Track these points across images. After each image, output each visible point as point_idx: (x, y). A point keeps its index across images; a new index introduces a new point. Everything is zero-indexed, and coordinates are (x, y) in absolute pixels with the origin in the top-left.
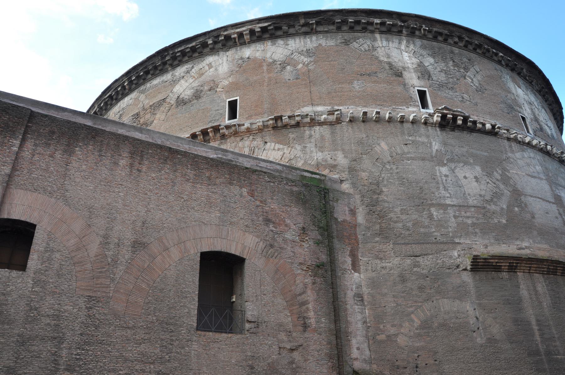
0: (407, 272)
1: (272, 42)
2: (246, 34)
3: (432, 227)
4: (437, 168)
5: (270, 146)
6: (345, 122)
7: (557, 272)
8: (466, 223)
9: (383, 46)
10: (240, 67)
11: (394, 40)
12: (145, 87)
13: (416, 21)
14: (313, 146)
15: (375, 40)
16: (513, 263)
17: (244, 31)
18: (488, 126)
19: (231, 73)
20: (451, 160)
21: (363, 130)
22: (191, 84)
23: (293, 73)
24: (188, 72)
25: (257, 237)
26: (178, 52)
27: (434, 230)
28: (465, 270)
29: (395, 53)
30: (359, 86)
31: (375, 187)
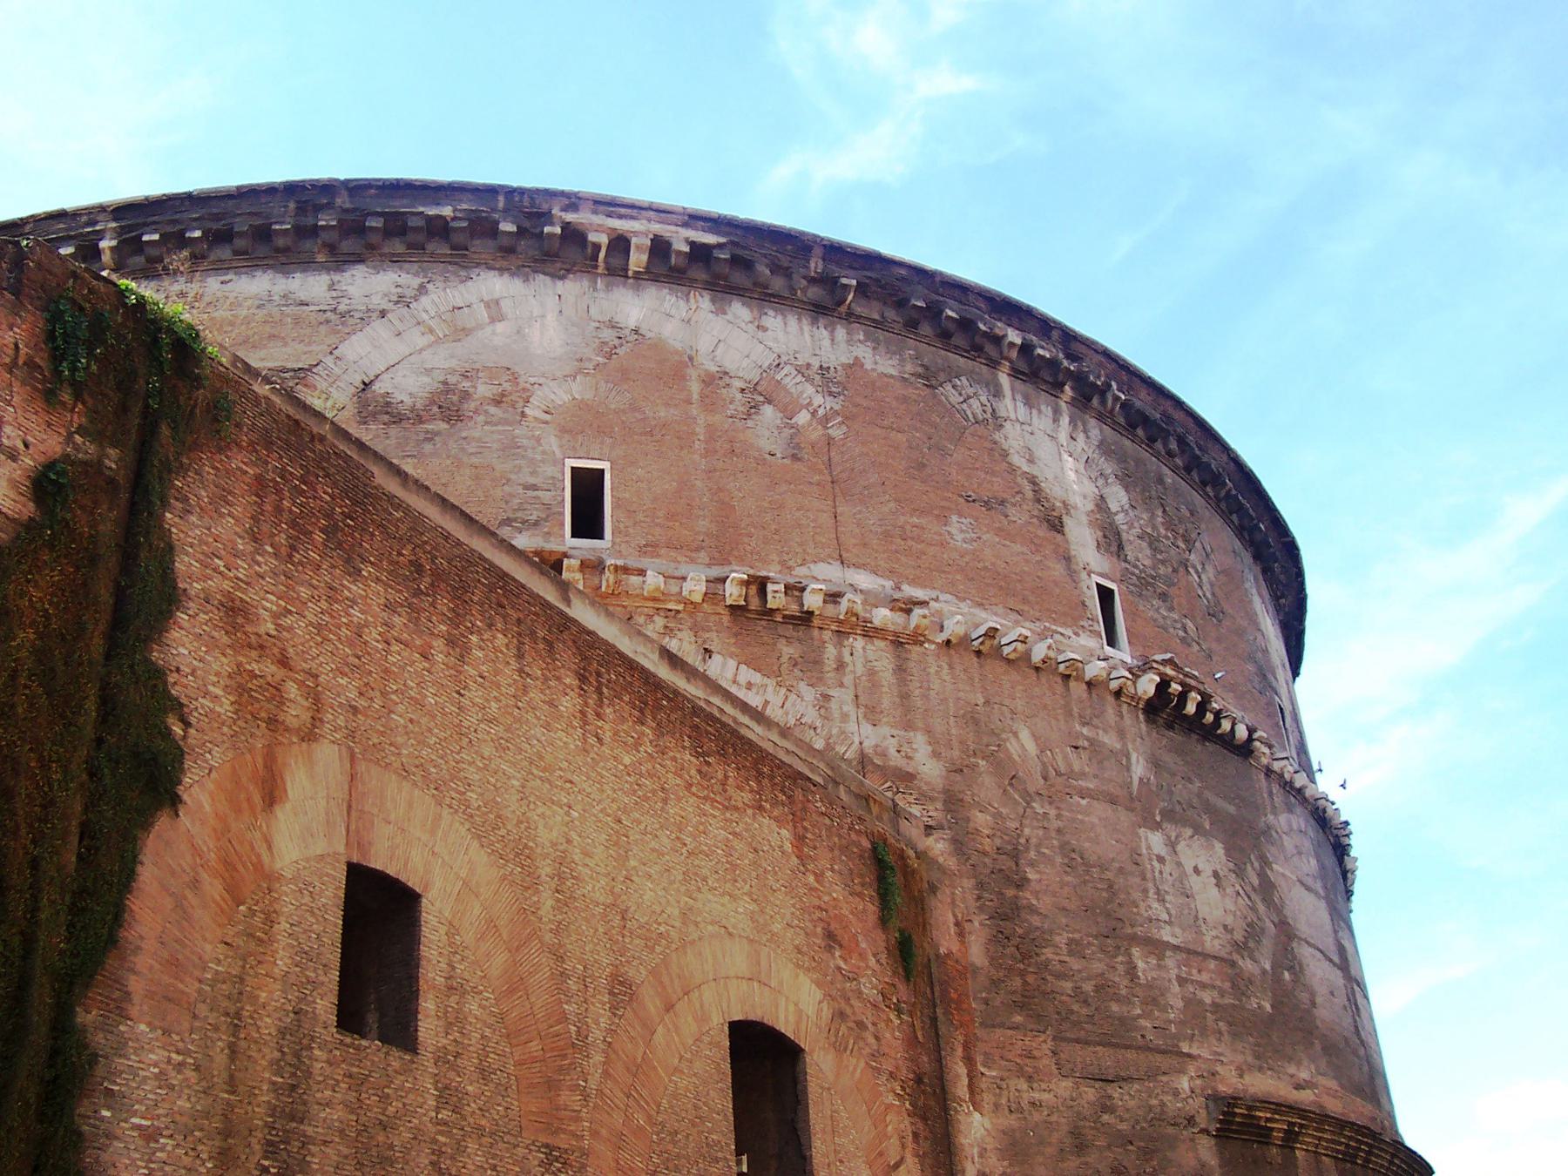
0: (1087, 1124)
1: (713, 301)
2: (637, 247)
3: (1134, 1004)
4: (1142, 831)
5: (724, 665)
6: (933, 642)
7: (1356, 1156)
8: (1201, 1002)
9: (1018, 420)
10: (609, 356)
11: (1043, 407)
13: (1100, 365)
14: (850, 701)
15: (997, 393)
16: (1294, 1124)
17: (635, 233)
18: (1242, 732)
20: (1169, 815)
21: (977, 680)
23: (783, 435)
24: (401, 301)
25: (818, 984)
29: (1044, 449)
30: (963, 536)
31: (1006, 863)
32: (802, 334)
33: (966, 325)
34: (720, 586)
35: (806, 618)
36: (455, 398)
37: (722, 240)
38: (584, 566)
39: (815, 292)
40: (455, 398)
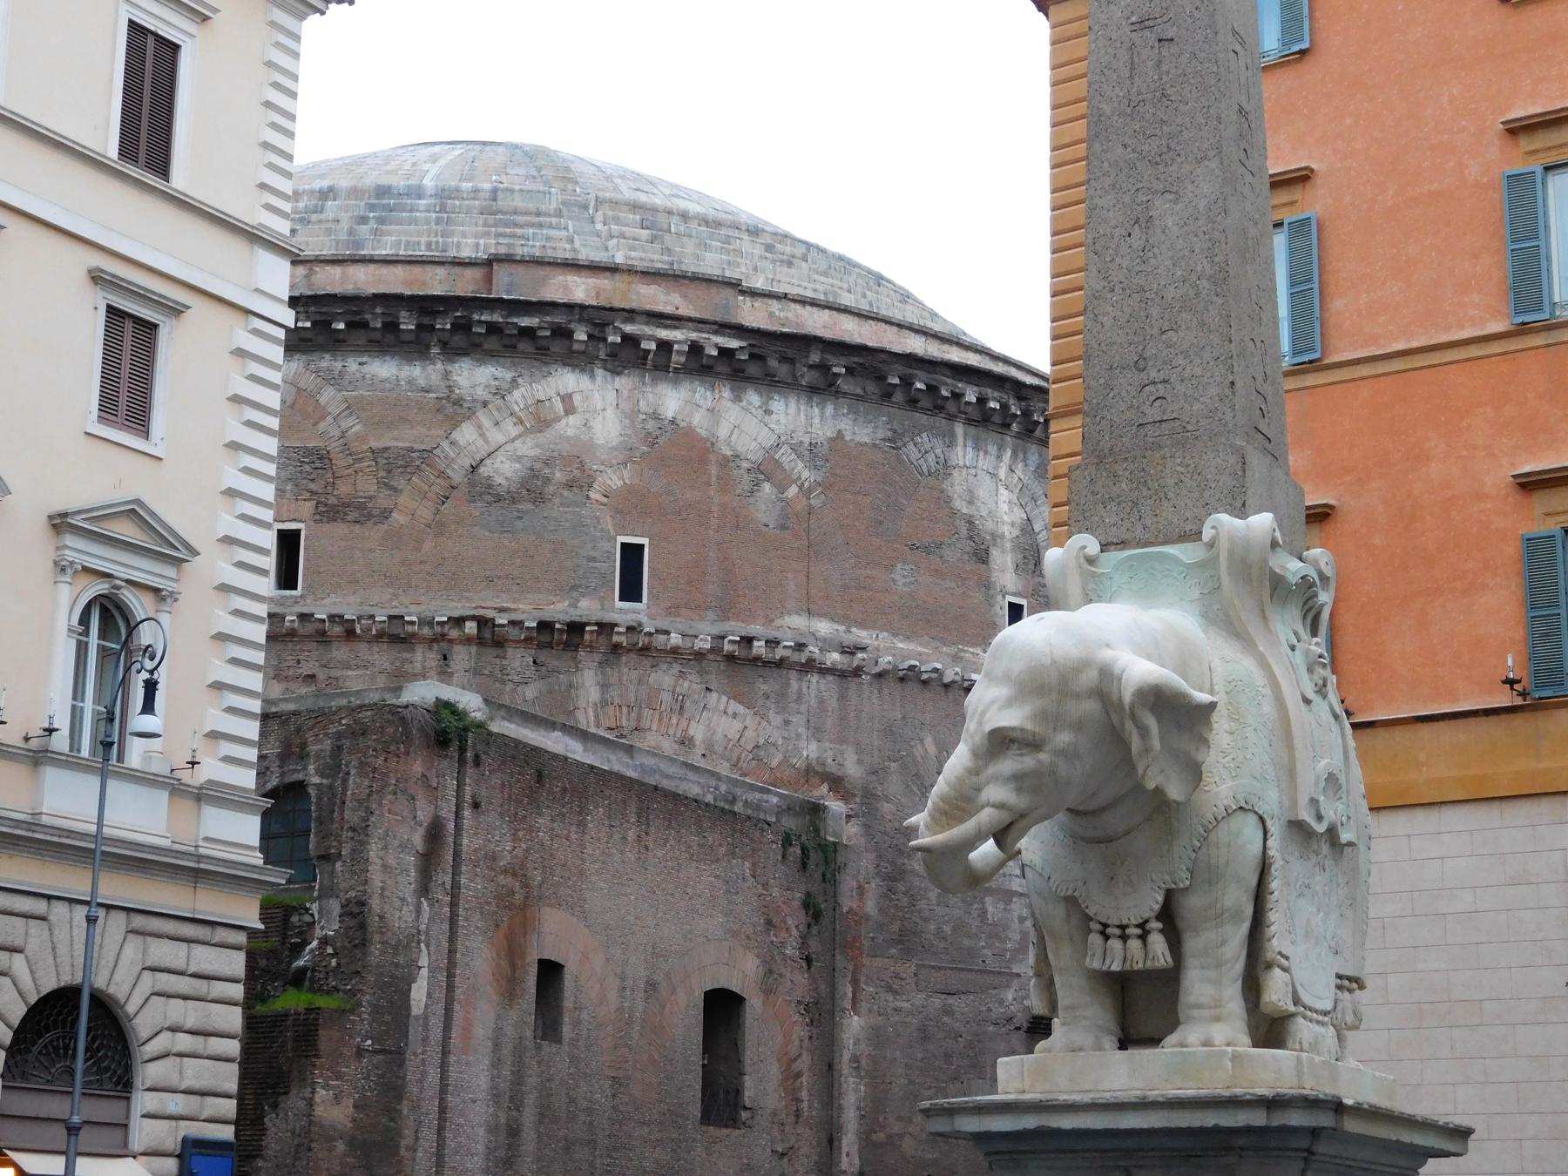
1: (732, 390)
2: (678, 352)
5: (718, 701)
12: (338, 365)
15: (951, 444)
17: (678, 342)
19: (628, 455)
22: (513, 440)
24: (500, 393)
26: (480, 322)
27: (983, 944)
28: (1018, 1029)
29: (984, 488)
30: (904, 581)
32: (799, 414)
33: (932, 389)
34: (720, 641)
35: (781, 664)
36: (539, 483)
37: (744, 344)
38: (630, 629)
39: (808, 377)
40: (539, 483)
